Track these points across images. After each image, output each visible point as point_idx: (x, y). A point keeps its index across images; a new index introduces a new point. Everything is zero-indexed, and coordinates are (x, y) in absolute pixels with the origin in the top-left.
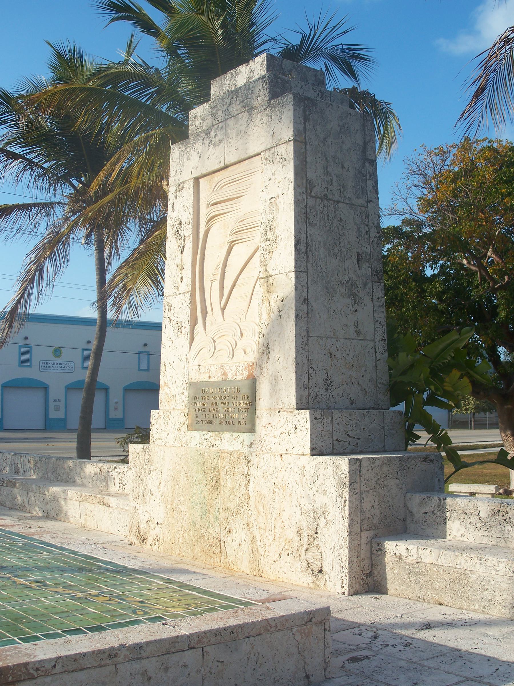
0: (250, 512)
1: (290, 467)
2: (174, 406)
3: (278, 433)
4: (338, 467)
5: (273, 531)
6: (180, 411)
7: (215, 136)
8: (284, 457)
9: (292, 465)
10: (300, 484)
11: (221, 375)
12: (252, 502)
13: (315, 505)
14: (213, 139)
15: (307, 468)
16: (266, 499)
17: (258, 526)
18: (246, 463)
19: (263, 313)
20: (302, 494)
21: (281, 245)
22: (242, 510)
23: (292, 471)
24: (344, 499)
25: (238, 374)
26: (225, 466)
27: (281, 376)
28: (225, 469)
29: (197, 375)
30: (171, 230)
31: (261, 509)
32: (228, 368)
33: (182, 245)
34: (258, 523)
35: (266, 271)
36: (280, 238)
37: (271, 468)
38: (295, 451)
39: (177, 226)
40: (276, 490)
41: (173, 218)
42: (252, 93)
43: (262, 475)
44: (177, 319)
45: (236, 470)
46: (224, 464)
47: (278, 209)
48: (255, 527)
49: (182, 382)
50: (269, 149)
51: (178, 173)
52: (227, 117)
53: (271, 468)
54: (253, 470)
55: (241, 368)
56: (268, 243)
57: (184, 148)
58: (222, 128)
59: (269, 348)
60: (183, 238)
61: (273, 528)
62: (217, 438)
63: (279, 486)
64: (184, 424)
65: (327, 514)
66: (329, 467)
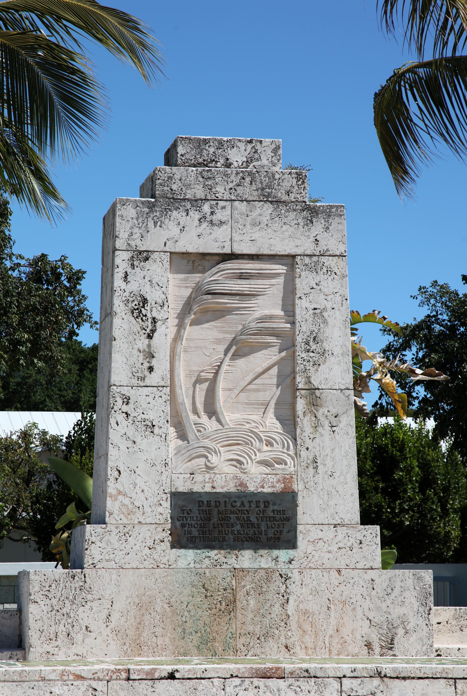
0: (289, 634)
1: (352, 581)
2: (141, 520)
3: (334, 548)
4: (420, 579)
5: (327, 649)
6: (154, 526)
7: (212, 213)
8: (343, 572)
9: (356, 579)
10: (367, 597)
11: (236, 486)
12: (293, 623)
13: (389, 616)
14: (207, 216)
15: (377, 581)
16: (315, 616)
17: (303, 646)
18: (283, 580)
19: (305, 425)
20: (371, 607)
21: (331, 360)
22: (277, 632)
23: (355, 586)
24: (428, 608)
25: (266, 487)
26: (244, 586)
27: (338, 492)
28: (245, 589)
29: (189, 484)
30: (122, 305)
31: (307, 627)
32: (248, 478)
33: (150, 327)
34: (302, 642)
35: (310, 382)
36: (330, 353)
37: (323, 585)
38: (359, 566)
39: (136, 302)
40: (332, 607)
41: (127, 291)
42: (279, 185)
43: (309, 592)
44: (143, 416)
45: (264, 590)
46: (243, 584)
47: (325, 322)
48: (298, 648)
49: (158, 492)
50: (310, 256)
51: (135, 236)
52: (233, 198)
53: (323, 585)
54: (292, 588)
55: (271, 480)
56: (312, 354)
57: (146, 210)
58: (224, 208)
59: (316, 462)
60: (150, 320)
61: (327, 645)
62: (229, 556)
63: (337, 602)
64: (162, 541)
65: (405, 624)
66: (407, 579)
